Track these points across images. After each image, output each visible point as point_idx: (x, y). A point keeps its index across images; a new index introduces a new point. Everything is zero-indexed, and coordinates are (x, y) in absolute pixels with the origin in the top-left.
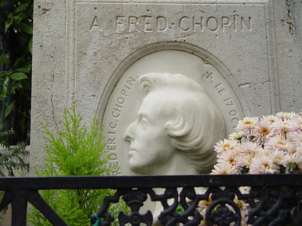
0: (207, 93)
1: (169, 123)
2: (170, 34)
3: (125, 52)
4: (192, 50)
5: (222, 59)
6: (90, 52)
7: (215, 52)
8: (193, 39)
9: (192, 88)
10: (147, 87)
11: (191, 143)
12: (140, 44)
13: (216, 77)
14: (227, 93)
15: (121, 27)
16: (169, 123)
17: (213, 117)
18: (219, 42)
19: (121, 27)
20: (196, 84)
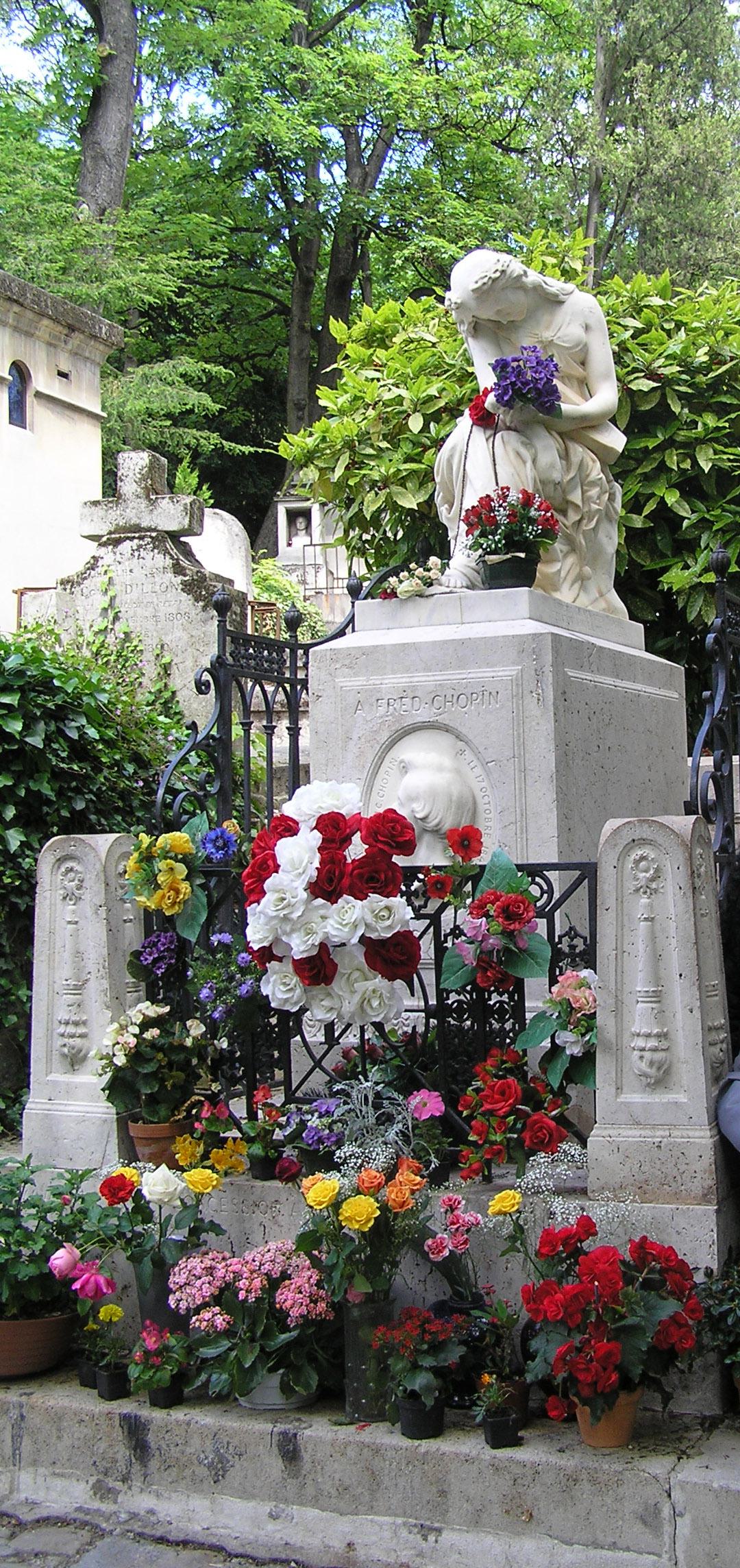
0: (458, 771)
1: (415, 806)
2: (424, 714)
3: (384, 736)
4: (447, 729)
5: (470, 737)
6: (355, 737)
7: (464, 730)
8: (444, 719)
9: (440, 769)
10: (405, 768)
11: (432, 824)
12: (397, 726)
13: (468, 755)
14: (479, 771)
15: (382, 710)
16: (415, 806)
17: (454, 798)
18: (467, 719)
19: (382, 710)
20: (447, 762)
